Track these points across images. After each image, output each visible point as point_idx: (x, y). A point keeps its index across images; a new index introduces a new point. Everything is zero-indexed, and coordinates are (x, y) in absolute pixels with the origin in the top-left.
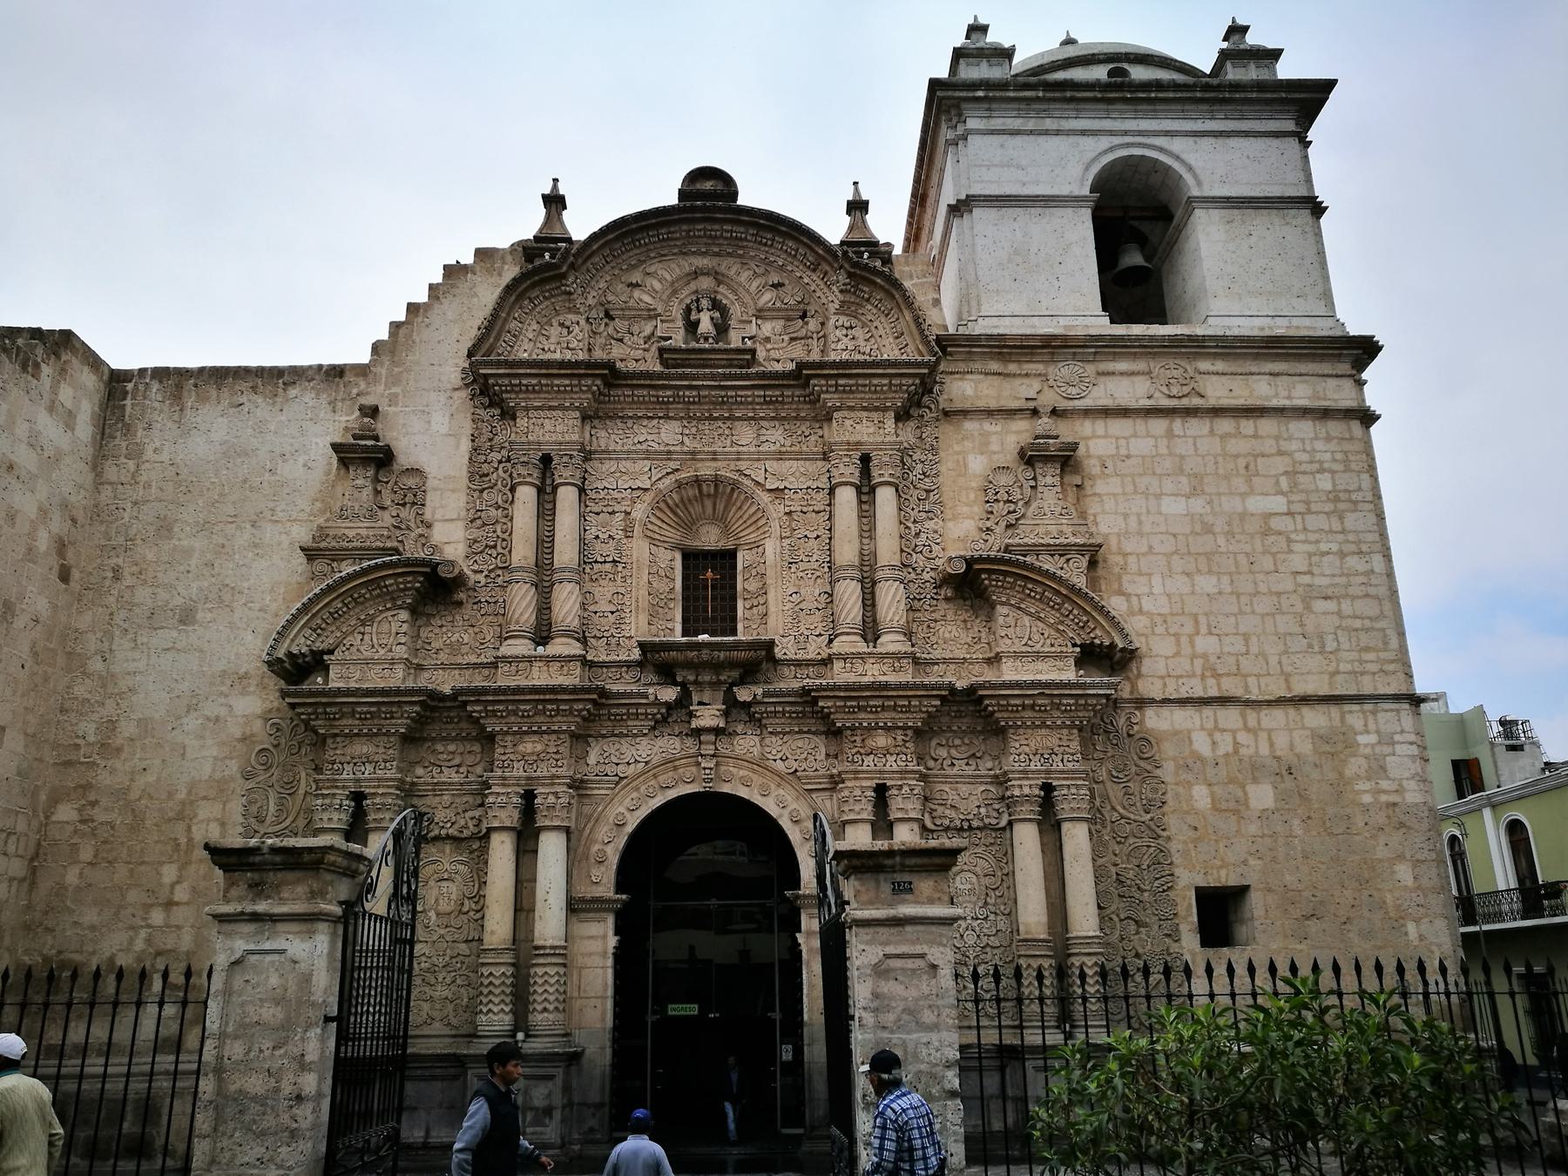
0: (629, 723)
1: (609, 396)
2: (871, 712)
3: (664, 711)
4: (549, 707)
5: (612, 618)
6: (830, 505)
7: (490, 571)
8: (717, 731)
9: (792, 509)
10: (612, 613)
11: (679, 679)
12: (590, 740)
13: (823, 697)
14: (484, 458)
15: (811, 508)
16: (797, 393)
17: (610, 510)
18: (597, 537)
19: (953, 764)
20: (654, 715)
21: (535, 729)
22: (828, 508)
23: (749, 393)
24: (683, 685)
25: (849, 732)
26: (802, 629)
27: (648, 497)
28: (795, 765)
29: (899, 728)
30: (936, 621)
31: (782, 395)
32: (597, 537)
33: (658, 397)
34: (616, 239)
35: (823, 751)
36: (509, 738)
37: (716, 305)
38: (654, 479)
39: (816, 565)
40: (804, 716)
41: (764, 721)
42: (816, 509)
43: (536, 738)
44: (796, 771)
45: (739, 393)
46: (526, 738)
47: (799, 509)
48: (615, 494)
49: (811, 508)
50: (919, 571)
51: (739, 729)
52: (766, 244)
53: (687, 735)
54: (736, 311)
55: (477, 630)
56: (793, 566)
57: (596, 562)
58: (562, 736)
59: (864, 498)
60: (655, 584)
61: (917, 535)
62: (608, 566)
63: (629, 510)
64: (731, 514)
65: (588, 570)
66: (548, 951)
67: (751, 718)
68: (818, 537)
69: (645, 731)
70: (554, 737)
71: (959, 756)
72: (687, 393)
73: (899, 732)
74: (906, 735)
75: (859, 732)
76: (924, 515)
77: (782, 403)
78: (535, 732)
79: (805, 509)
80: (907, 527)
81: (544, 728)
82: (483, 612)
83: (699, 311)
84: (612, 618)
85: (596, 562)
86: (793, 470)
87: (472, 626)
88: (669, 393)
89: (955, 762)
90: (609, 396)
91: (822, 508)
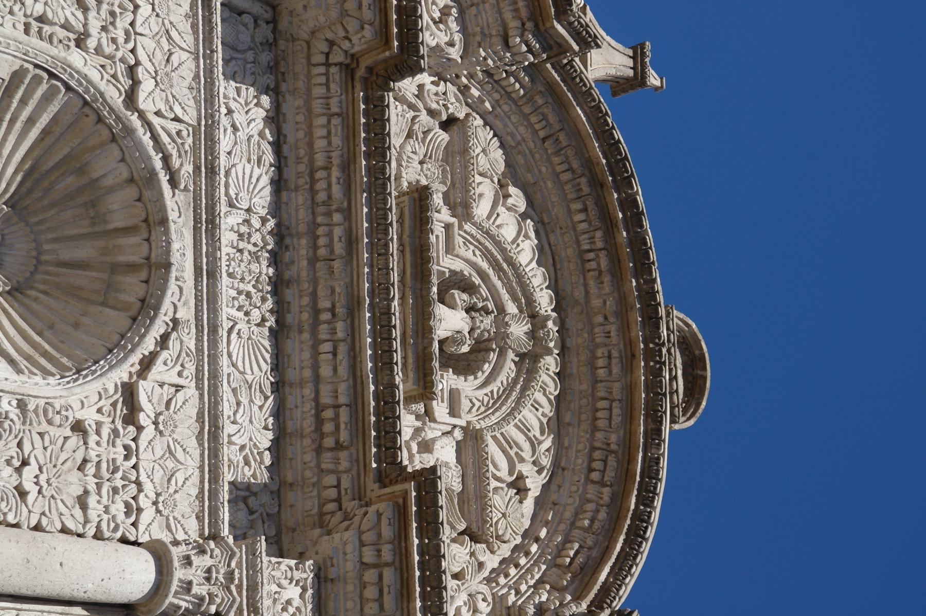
1: (327, 64)
9: (93, 438)
15: (92, 487)
16: (346, 483)
23: (343, 371)
27: (115, 97)
31: (339, 446)
33: (327, 168)
34: (589, 164)
37: (481, 348)
38: (156, 121)
42: (92, 501)
45: (342, 349)
47: (92, 454)
48: (122, 23)
49: (92, 487)
52: (591, 470)
54: (467, 386)
63: (92, 43)
68: (22, 494)
72: (338, 232)
77: (319, 450)
79: (91, 469)
83: (468, 311)
86: (180, 454)
88: (336, 190)
90: (327, 64)
91: (93, 514)
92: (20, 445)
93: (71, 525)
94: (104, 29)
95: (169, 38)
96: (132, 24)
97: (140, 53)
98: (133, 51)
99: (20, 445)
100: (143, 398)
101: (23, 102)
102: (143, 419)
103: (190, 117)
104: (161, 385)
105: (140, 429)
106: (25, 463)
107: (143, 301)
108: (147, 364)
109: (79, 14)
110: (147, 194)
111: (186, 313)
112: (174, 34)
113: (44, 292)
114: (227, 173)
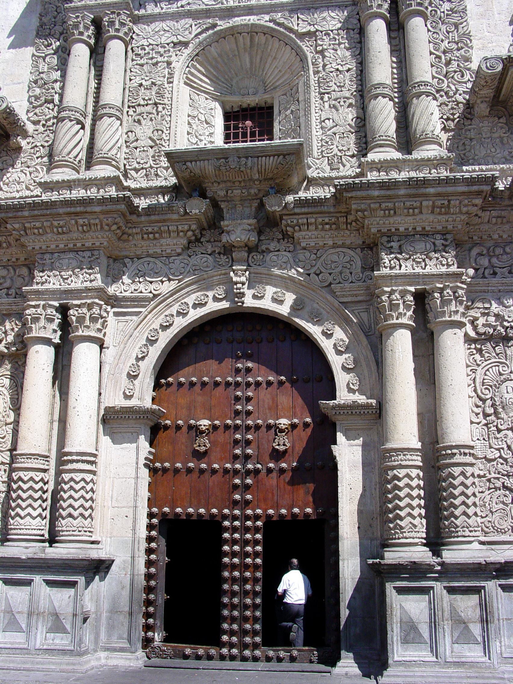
0: (163, 241)
2: (408, 215)
3: (194, 227)
4: (81, 221)
5: (151, 152)
6: (360, 42)
7: (46, 121)
8: (251, 249)
10: (152, 147)
11: (209, 194)
12: (127, 260)
13: (356, 198)
14: (48, 31)
17: (154, 61)
18: (141, 85)
19: (495, 274)
20: (185, 232)
21: (71, 246)
22: (358, 45)
24: (215, 204)
25: (385, 239)
26: (336, 151)
28: (330, 279)
29: (438, 233)
30: (471, 139)
32: (141, 85)
35: (359, 264)
36: (47, 256)
39: (348, 94)
40: (338, 228)
41: (296, 235)
43: (71, 255)
44: (330, 284)
46: (63, 256)
50: (451, 93)
51: (273, 246)
53: (219, 253)
55: (31, 169)
56: (326, 96)
57: (139, 105)
58: (96, 253)
59: (393, 35)
60: (194, 126)
61: (448, 63)
62: (149, 108)
64: (267, 66)
65: (131, 113)
66: (75, 458)
67: (285, 236)
69: (179, 251)
70: (88, 254)
71: (500, 264)
73: (438, 236)
74: (446, 240)
75: (396, 238)
76: (454, 46)
78: (71, 251)
80: (439, 57)
81: (79, 245)
82: (38, 154)
84: (151, 152)
85: (139, 105)
87: (28, 167)
89: (497, 270)
92: (332, 72)
93: (358, 52)
94: (161, 56)
95: (159, 31)
96: (157, 45)
97: (168, 42)
98: (168, 44)
99: (332, 72)
100: (304, 30)
101: (195, 83)
102: (312, 29)
103: (190, 21)
104: (298, 24)
105: (317, 31)
106: (337, 70)
107: (265, 34)
108: (291, 30)
109: (160, 64)
110: (223, 35)
111: (267, 17)
112: (157, 30)
113: (263, 71)
114: (206, 5)
